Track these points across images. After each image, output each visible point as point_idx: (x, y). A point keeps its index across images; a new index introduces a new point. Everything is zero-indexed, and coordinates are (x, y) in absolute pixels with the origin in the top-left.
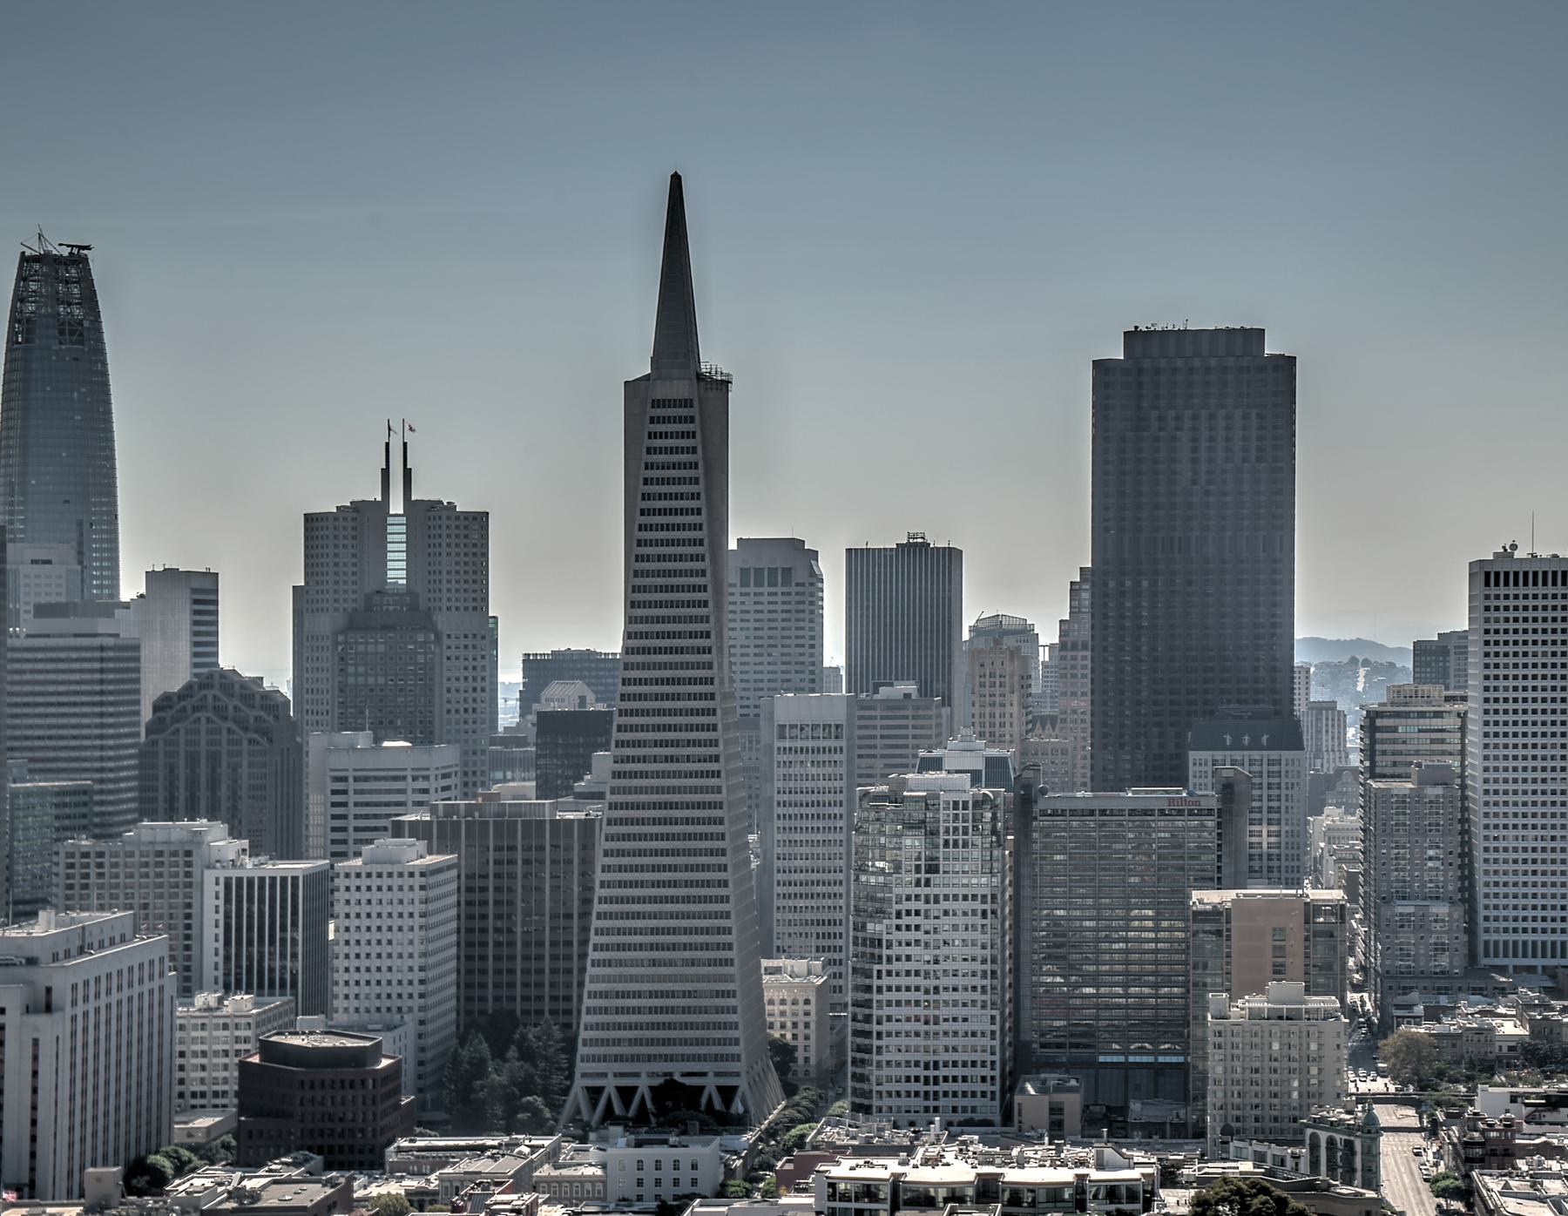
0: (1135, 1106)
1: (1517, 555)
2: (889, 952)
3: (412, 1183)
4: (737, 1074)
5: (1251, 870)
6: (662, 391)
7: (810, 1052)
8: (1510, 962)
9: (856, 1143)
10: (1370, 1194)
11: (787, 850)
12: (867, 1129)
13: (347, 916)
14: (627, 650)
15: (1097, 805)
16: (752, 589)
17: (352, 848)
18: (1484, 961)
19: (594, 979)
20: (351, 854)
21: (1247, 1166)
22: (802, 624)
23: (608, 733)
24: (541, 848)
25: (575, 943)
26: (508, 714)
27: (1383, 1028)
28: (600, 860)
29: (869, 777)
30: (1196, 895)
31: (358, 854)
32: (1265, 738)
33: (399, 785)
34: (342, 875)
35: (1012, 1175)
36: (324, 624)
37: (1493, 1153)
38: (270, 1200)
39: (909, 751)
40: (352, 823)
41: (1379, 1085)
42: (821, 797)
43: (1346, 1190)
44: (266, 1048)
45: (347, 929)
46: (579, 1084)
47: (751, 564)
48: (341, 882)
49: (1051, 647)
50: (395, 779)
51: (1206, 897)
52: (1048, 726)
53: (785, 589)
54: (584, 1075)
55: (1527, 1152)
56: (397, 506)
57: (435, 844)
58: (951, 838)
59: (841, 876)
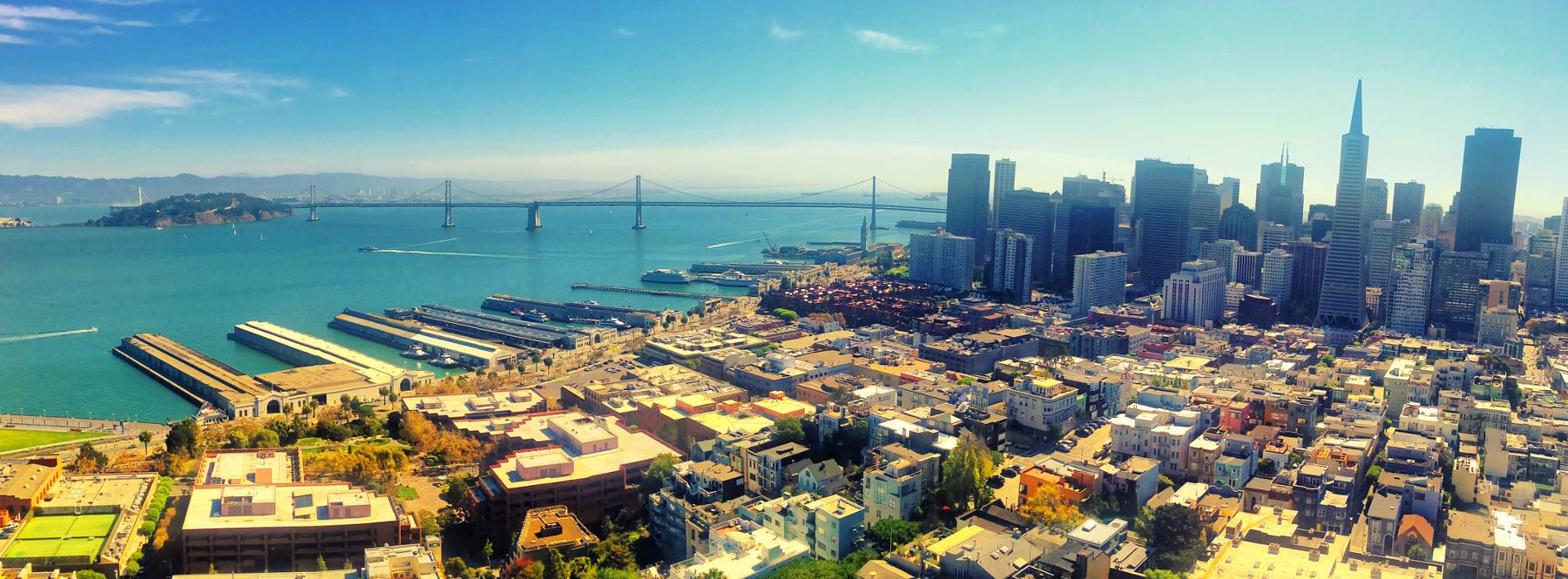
0: (1459, 333)
3: (1278, 334)
7: (1376, 311)
8: (1563, 304)
12: (1390, 332)
21: (1488, 351)
26: (1305, 218)
27: (1525, 320)
28: (1327, 258)
29: (1398, 244)
30: (1481, 281)
35: (1429, 347)
38: (1246, 333)
40: (1268, 244)
41: (1524, 334)
44: (1246, 297)
46: (1319, 314)
48: (1265, 259)
51: (1483, 281)
55: (1562, 353)
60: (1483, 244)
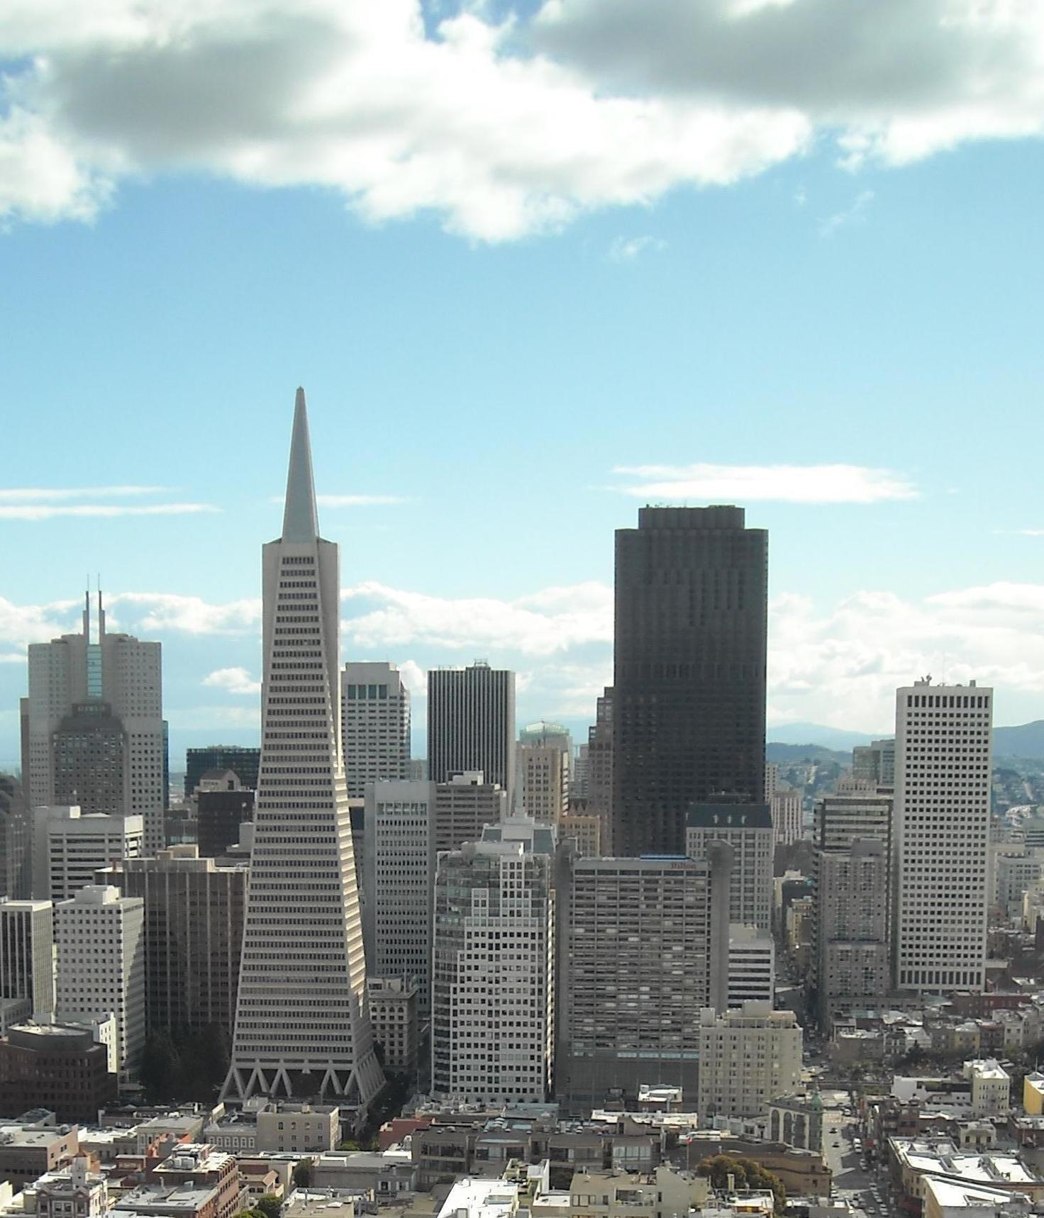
1: (932, 684)
2: (462, 974)
4: (351, 1062)
5: (731, 917)
6: (290, 552)
9: (438, 1113)
10: (815, 1154)
11: (386, 897)
13: (66, 941)
14: (266, 747)
15: (618, 867)
16: (357, 701)
17: (67, 892)
18: (901, 986)
19: (244, 991)
20: (66, 896)
21: (726, 1134)
22: (394, 728)
23: (249, 808)
24: (203, 894)
25: (230, 965)
31: (72, 896)
32: (743, 819)
33: (99, 846)
34: (61, 912)
36: (42, 727)
37: (903, 1124)
39: (476, 824)
40: (67, 873)
42: (410, 858)
43: (799, 1151)
45: (66, 951)
47: (356, 682)
49: (582, 748)
50: (96, 841)
52: (580, 807)
53: (383, 701)
54: (238, 1060)
56: (94, 638)
57: (126, 890)
58: (509, 890)
59: (426, 918)
60: (689, 830)
